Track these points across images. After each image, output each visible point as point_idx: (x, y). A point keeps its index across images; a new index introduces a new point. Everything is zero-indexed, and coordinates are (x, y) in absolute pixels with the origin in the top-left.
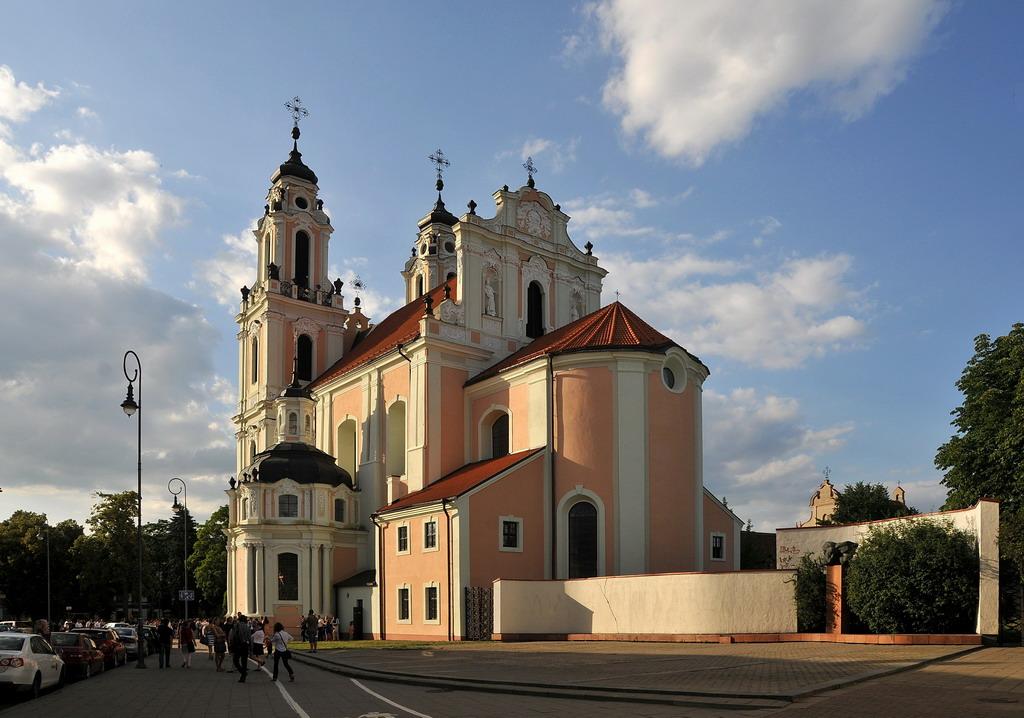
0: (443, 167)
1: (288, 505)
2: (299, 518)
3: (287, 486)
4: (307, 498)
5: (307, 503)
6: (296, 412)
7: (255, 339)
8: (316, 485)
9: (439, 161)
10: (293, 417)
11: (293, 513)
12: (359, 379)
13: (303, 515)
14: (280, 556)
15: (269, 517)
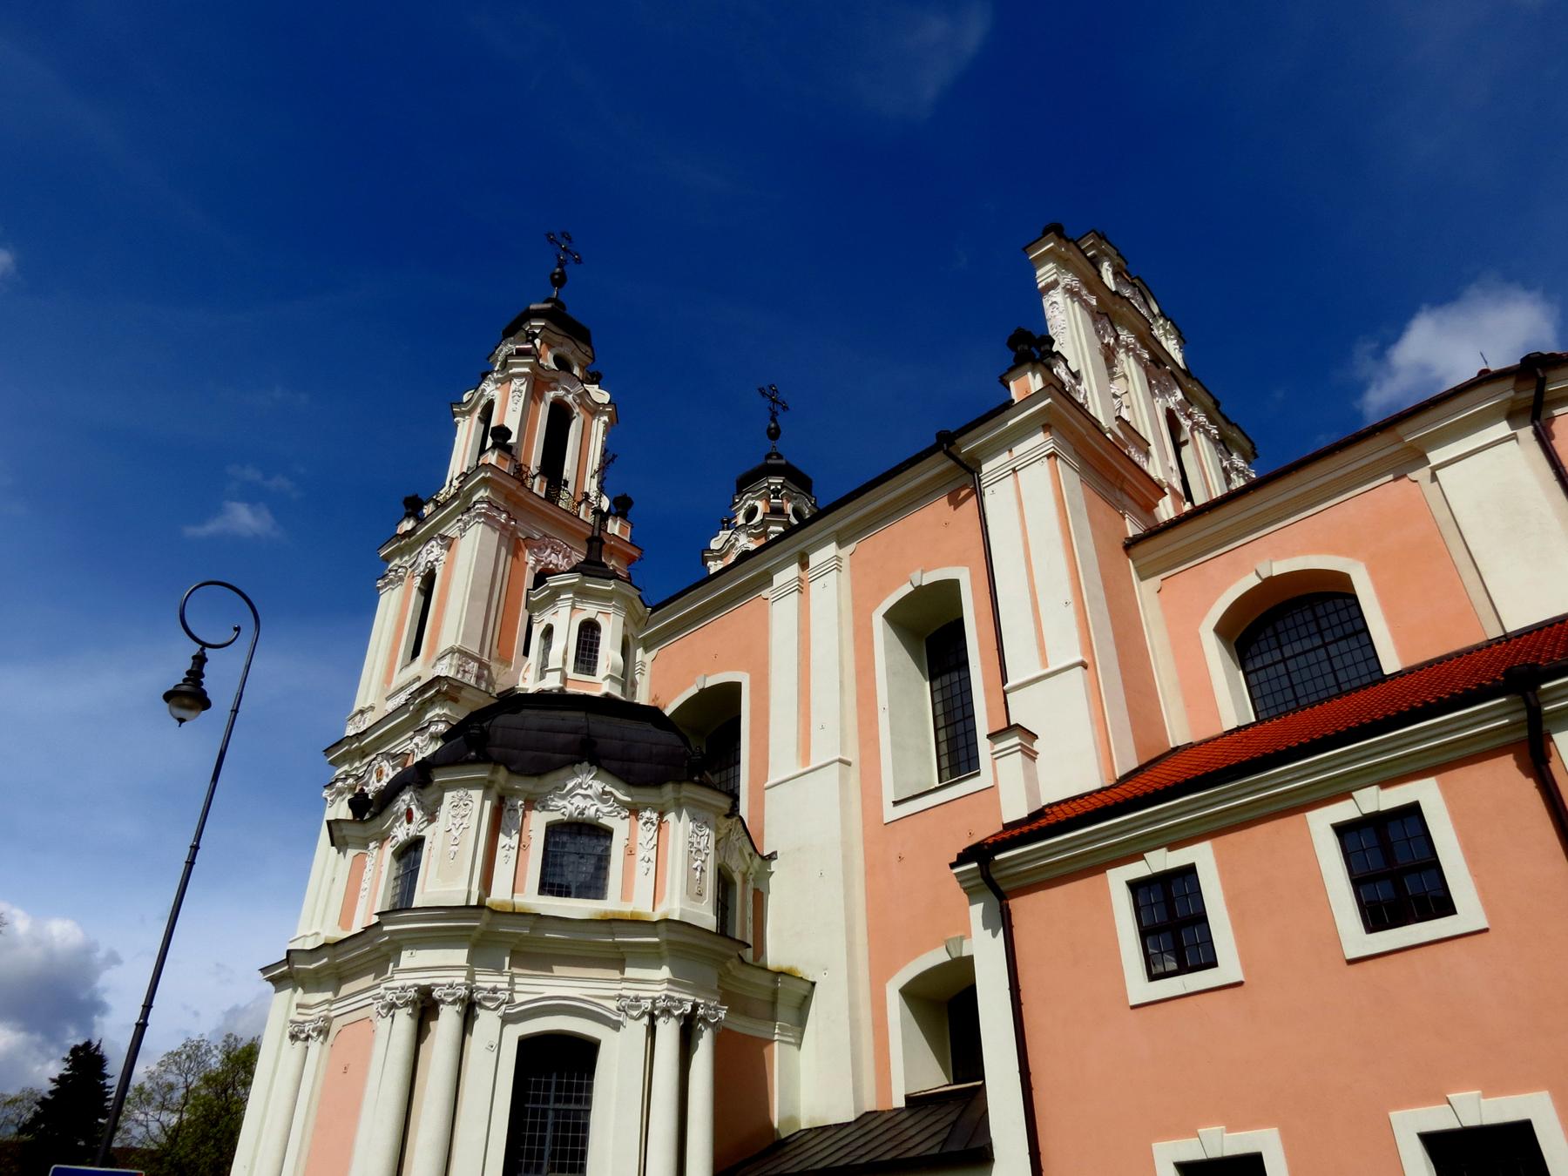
0: (778, 408)
1: (576, 855)
2: (612, 903)
3: (585, 794)
4: (645, 835)
5: (645, 851)
6: (601, 619)
7: (429, 580)
8: (689, 791)
9: (774, 401)
10: (589, 633)
11: (595, 887)
12: (765, 580)
13: (626, 894)
14: (527, 1046)
15: (500, 893)
